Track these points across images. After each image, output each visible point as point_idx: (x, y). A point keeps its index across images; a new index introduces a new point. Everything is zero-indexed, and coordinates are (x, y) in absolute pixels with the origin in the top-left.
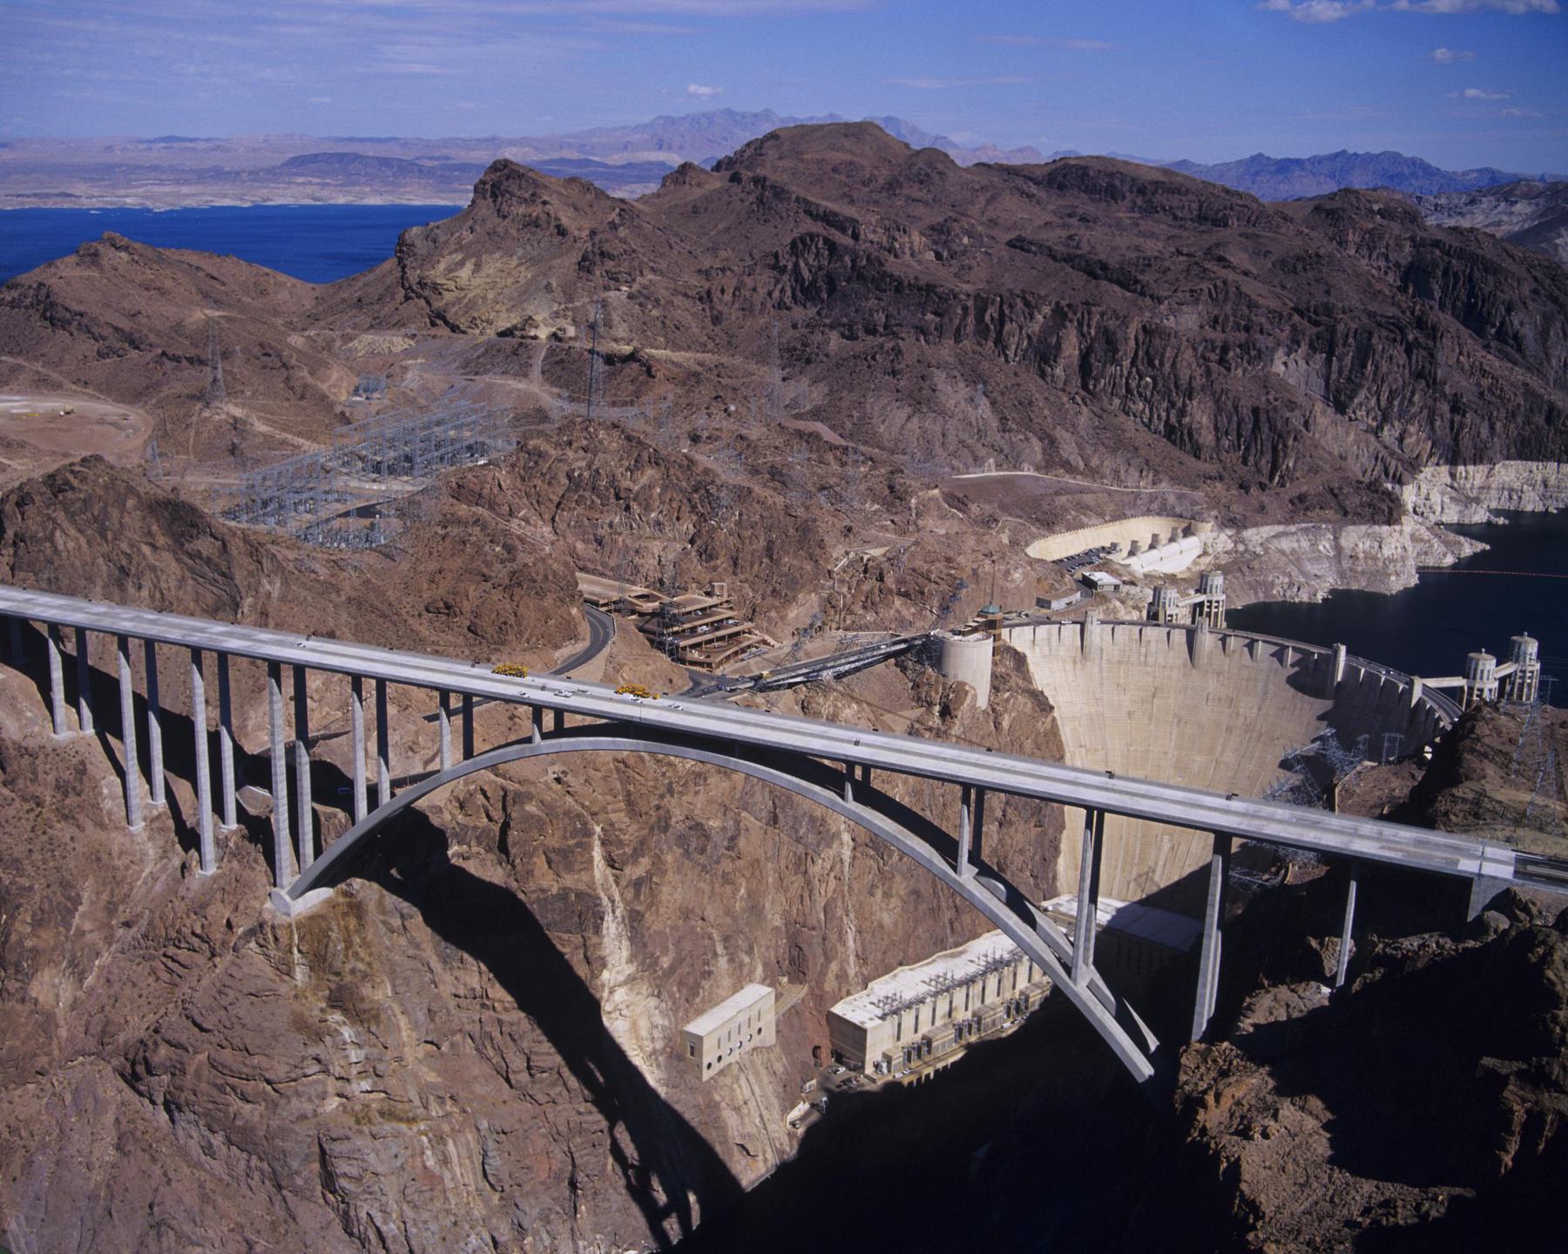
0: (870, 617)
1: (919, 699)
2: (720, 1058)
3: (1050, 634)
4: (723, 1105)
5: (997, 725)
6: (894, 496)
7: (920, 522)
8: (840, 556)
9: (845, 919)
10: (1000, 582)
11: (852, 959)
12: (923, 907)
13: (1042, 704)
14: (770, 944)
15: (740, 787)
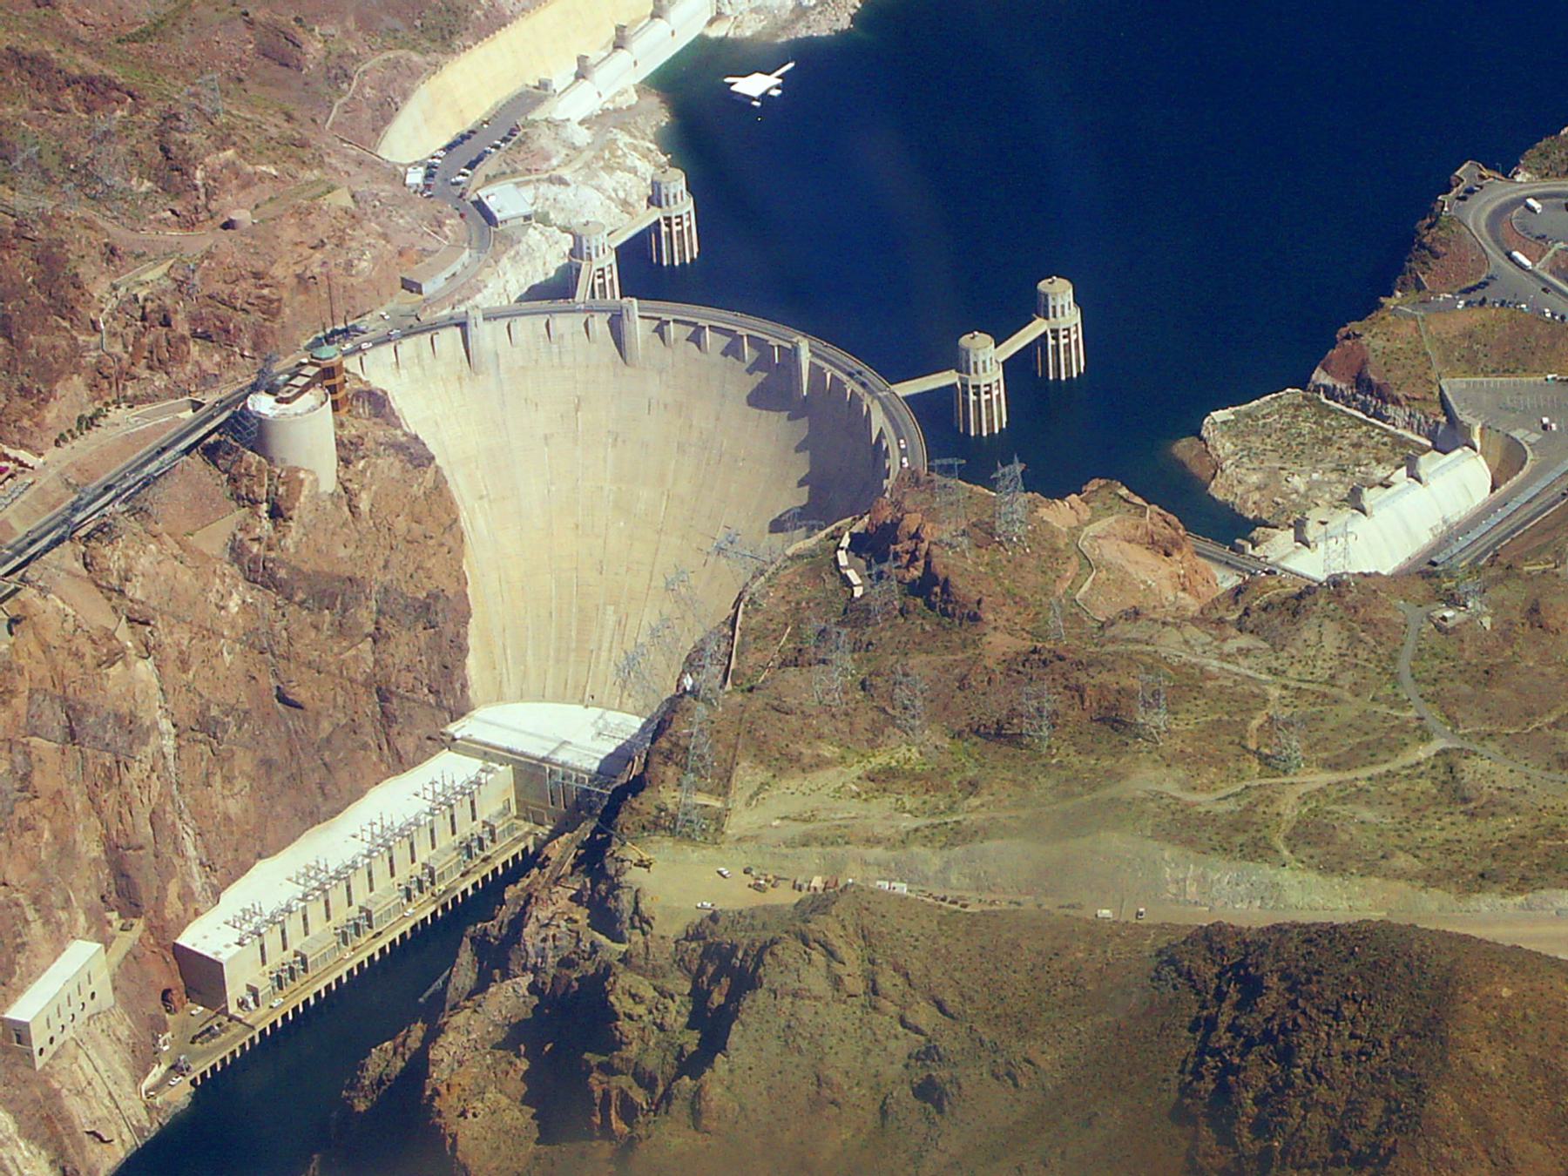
0: (160, 381)
1: (240, 498)
2: (52, 1040)
3: (417, 345)
4: (64, 1092)
5: (353, 509)
6: (172, 169)
7: (213, 205)
8: (103, 292)
9: (179, 825)
10: (341, 280)
11: (195, 869)
12: (277, 778)
13: (416, 455)
14: (87, 882)
15: (23, 711)
